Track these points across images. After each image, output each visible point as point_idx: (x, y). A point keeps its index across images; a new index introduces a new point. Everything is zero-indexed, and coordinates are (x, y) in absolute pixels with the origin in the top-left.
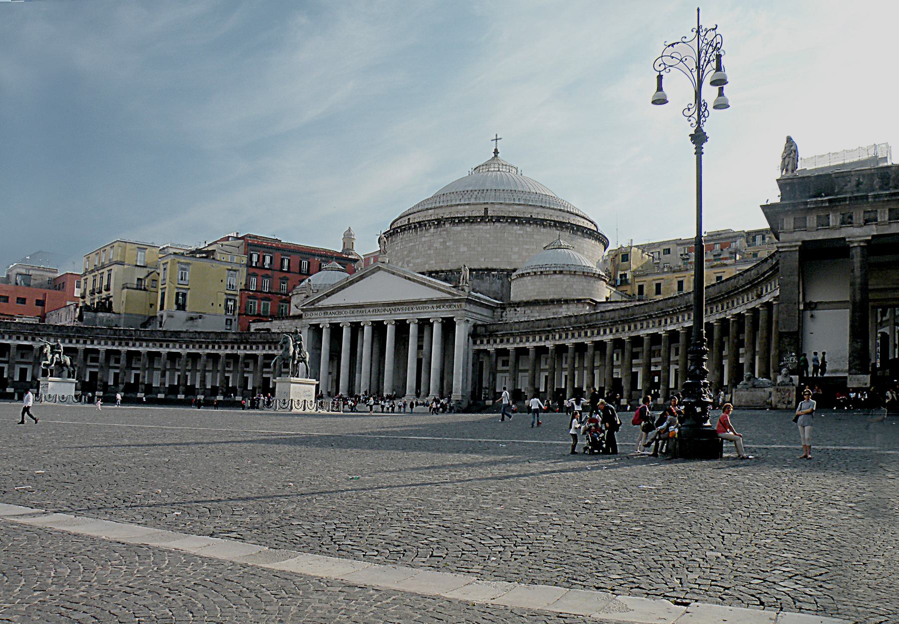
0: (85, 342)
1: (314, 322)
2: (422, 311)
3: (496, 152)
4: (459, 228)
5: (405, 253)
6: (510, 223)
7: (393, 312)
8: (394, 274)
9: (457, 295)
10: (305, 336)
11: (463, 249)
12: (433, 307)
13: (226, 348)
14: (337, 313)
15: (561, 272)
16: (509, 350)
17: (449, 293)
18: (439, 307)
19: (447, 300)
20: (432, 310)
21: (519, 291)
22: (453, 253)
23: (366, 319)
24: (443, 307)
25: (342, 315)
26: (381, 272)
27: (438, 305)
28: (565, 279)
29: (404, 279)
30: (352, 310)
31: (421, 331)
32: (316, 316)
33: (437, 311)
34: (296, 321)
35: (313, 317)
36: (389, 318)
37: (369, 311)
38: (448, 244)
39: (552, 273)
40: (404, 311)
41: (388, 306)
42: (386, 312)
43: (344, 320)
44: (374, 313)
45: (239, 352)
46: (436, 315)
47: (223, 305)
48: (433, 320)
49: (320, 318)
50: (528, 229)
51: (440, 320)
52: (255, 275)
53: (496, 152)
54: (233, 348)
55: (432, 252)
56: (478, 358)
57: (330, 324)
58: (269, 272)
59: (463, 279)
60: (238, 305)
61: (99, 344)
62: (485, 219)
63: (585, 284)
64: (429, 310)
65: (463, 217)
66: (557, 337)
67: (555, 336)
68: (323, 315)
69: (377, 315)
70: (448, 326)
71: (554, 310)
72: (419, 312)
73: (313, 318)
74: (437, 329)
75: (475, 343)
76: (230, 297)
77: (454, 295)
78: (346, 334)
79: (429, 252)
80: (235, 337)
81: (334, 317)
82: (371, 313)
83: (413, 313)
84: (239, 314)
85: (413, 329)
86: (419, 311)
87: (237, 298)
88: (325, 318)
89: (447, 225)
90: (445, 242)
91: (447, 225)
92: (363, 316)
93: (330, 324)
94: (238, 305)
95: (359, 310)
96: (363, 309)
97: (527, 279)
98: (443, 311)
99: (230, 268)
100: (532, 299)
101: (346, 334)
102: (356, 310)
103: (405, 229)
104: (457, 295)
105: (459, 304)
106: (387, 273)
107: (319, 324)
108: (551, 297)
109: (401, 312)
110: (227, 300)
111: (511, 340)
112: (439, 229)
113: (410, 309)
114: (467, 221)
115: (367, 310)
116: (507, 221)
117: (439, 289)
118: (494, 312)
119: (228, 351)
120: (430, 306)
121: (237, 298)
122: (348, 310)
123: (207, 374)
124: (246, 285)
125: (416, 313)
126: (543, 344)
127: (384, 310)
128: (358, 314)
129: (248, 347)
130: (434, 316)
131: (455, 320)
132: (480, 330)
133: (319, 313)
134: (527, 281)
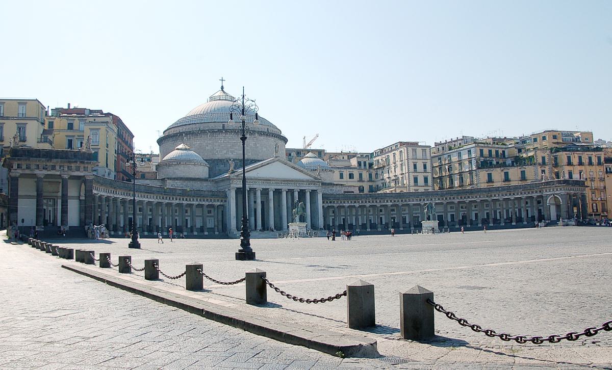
3: (222, 88)
4: (262, 138)
5: (229, 146)
8: (285, 164)
11: (264, 149)
13: (176, 200)
23: (272, 187)
34: (186, 182)
36: (285, 188)
38: (257, 145)
45: (183, 202)
46: (308, 188)
53: (222, 88)
55: (249, 148)
66: (360, 202)
70: (313, 193)
71: (331, 188)
80: (180, 192)
89: (256, 135)
90: (255, 144)
106: (281, 163)
119: (178, 202)
120: (305, 183)
126: (353, 205)
129: (188, 199)
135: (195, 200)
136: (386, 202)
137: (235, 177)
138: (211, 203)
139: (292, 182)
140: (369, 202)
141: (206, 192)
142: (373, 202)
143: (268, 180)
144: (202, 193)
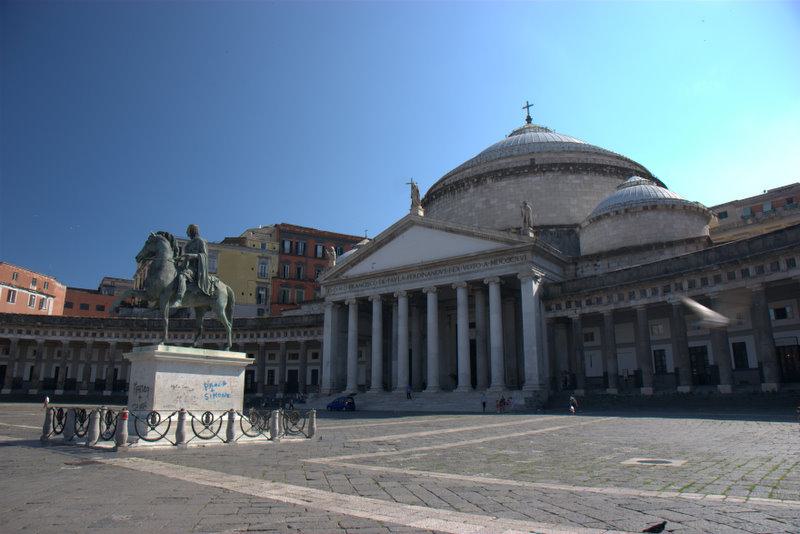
0: (94, 335)
1: (338, 298)
3: (529, 120)
4: (503, 183)
6: (563, 172)
8: (431, 227)
9: (519, 243)
10: (329, 317)
13: (245, 336)
15: (654, 207)
16: (602, 315)
17: (508, 242)
18: (495, 262)
21: (589, 242)
22: (499, 213)
23: (401, 288)
26: (415, 227)
28: (661, 217)
29: (444, 233)
31: (471, 297)
33: (492, 269)
36: (427, 284)
37: (403, 278)
38: (492, 202)
39: (641, 209)
43: (373, 292)
46: (490, 273)
47: (254, 294)
50: (586, 178)
51: (498, 280)
52: (289, 262)
53: (529, 120)
54: (252, 336)
56: (557, 328)
58: (303, 260)
60: (270, 293)
61: (109, 336)
62: (533, 168)
63: (688, 222)
65: (508, 169)
67: (681, 284)
70: (511, 289)
72: (468, 273)
74: (494, 293)
75: (548, 309)
76: (261, 285)
77: (514, 243)
78: (377, 309)
79: (470, 215)
80: (254, 324)
84: (272, 304)
85: (461, 296)
87: (269, 286)
89: (489, 181)
90: (487, 201)
91: (489, 181)
94: (270, 293)
97: (606, 224)
99: (260, 254)
100: (617, 247)
101: (377, 309)
103: (440, 194)
104: (519, 243)
106: (422, 228)
108: (644, 241)
110: (258, 289)
111: (605, 300)
112: (480, 188)
114: (511, 174)
116: (560, 169)
117: (493, 239)
118: (564, 270)
121: (269, 286)
123: (92, 366)
124: (278, 273)
125: (463, 273)
126: (660, 299)
129: (269, 334)
132: (557, 290)
134: (606, 226)
135: (282, 334)
136: (783, 266)
138: (311, 338)
139: (447, 267)
140: (718, 280)
141: (306, 319)
142: (731, 277)
143: (390, 275)
144: (296, 321)
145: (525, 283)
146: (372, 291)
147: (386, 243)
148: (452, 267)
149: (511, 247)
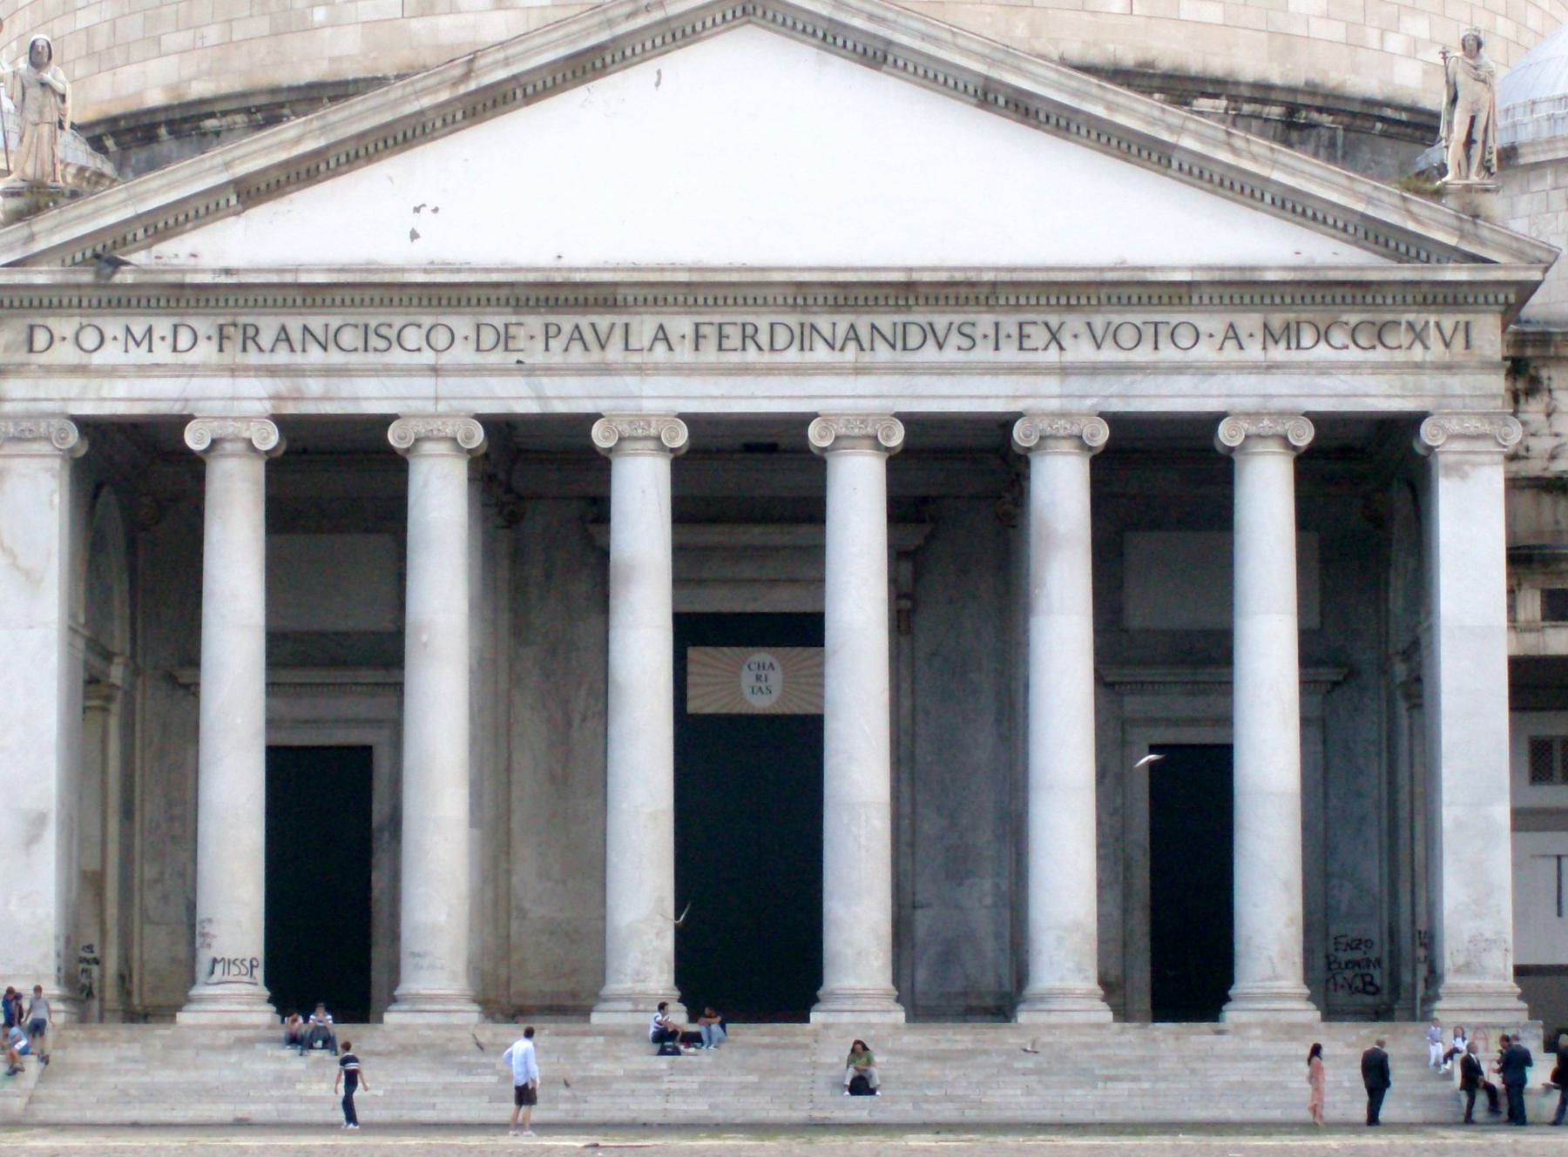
2: (1143, 354)
7: (883, 353)
12: (1232, 333)
14: (349, 338)
17: (1374, 234)
18: (1290, 334)
19: (1356, 290)
20: (1231, 353)
24: (1323, 335)
25: (397, 357)
27: (1277, 320)
30: (499, 321)
32: (139, 355)
33: (1271, 368)
35: (111, 354)
37: (662, 335)
40: (984, 353)
41: (837, 307)
42: (821, 353)
44: (709, 354)
48: (1246, 426)
49: (191, 370)
51: (1304, 436)
57: (283, 422)
59: (1469, 142)
64: (1205, 352)
68: (206, 352)
69: (745, 370)
73: (112, 372)
81: (328, 372)
82: (684, 354)
83: (1065, 371)
86: (1109, 354)
88: (234, 371)
92: (606, 369)
93: (281, 421)
95: (567, 322)
96: (603, 321)
98: (1324, 369)
102: (534, 323)
105: (1448, 322)
107: (184, 420)
109: (950, 355)
113: (1038, 336)
115: (645, 326)
120: (1212, 323)
122: (462, 325)
125: (1094, 370)
127: (804, 337)
128: (556, 357)
130: (1250, 404)
131: (1428, 433)
133: (163, 326)
137: (40, 276)
145: (1457, 470)
146: (425, 385)
147: (529, 99)
148: (1010, 323)
149: (1406, 273)
